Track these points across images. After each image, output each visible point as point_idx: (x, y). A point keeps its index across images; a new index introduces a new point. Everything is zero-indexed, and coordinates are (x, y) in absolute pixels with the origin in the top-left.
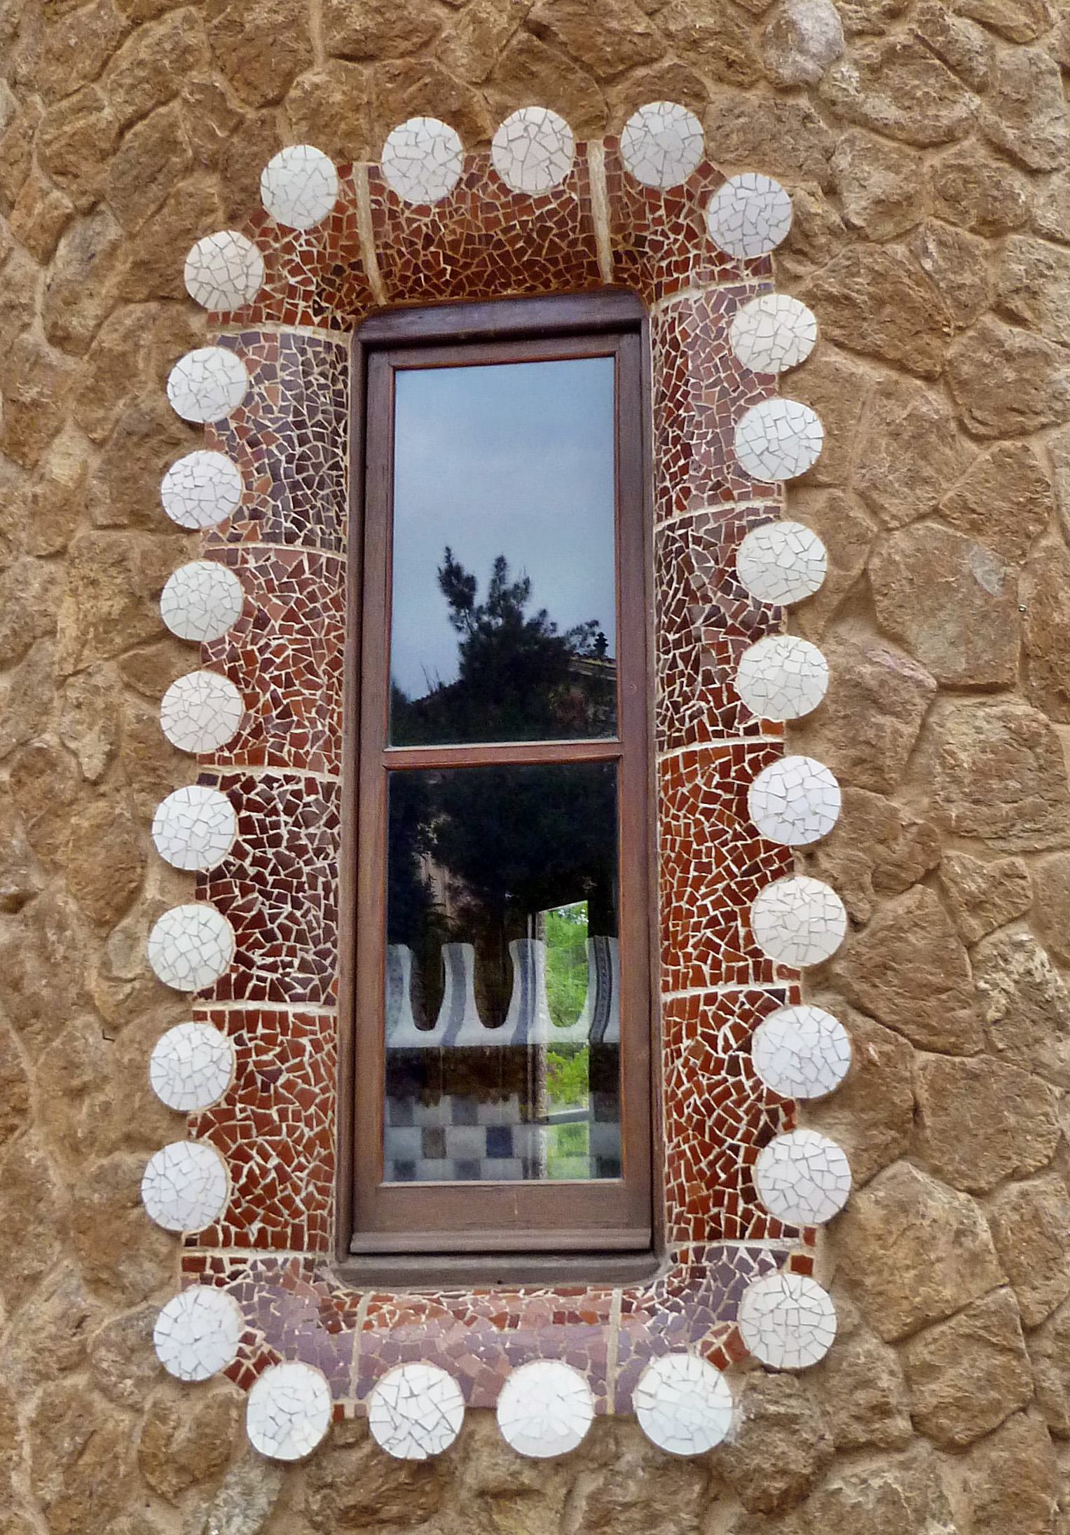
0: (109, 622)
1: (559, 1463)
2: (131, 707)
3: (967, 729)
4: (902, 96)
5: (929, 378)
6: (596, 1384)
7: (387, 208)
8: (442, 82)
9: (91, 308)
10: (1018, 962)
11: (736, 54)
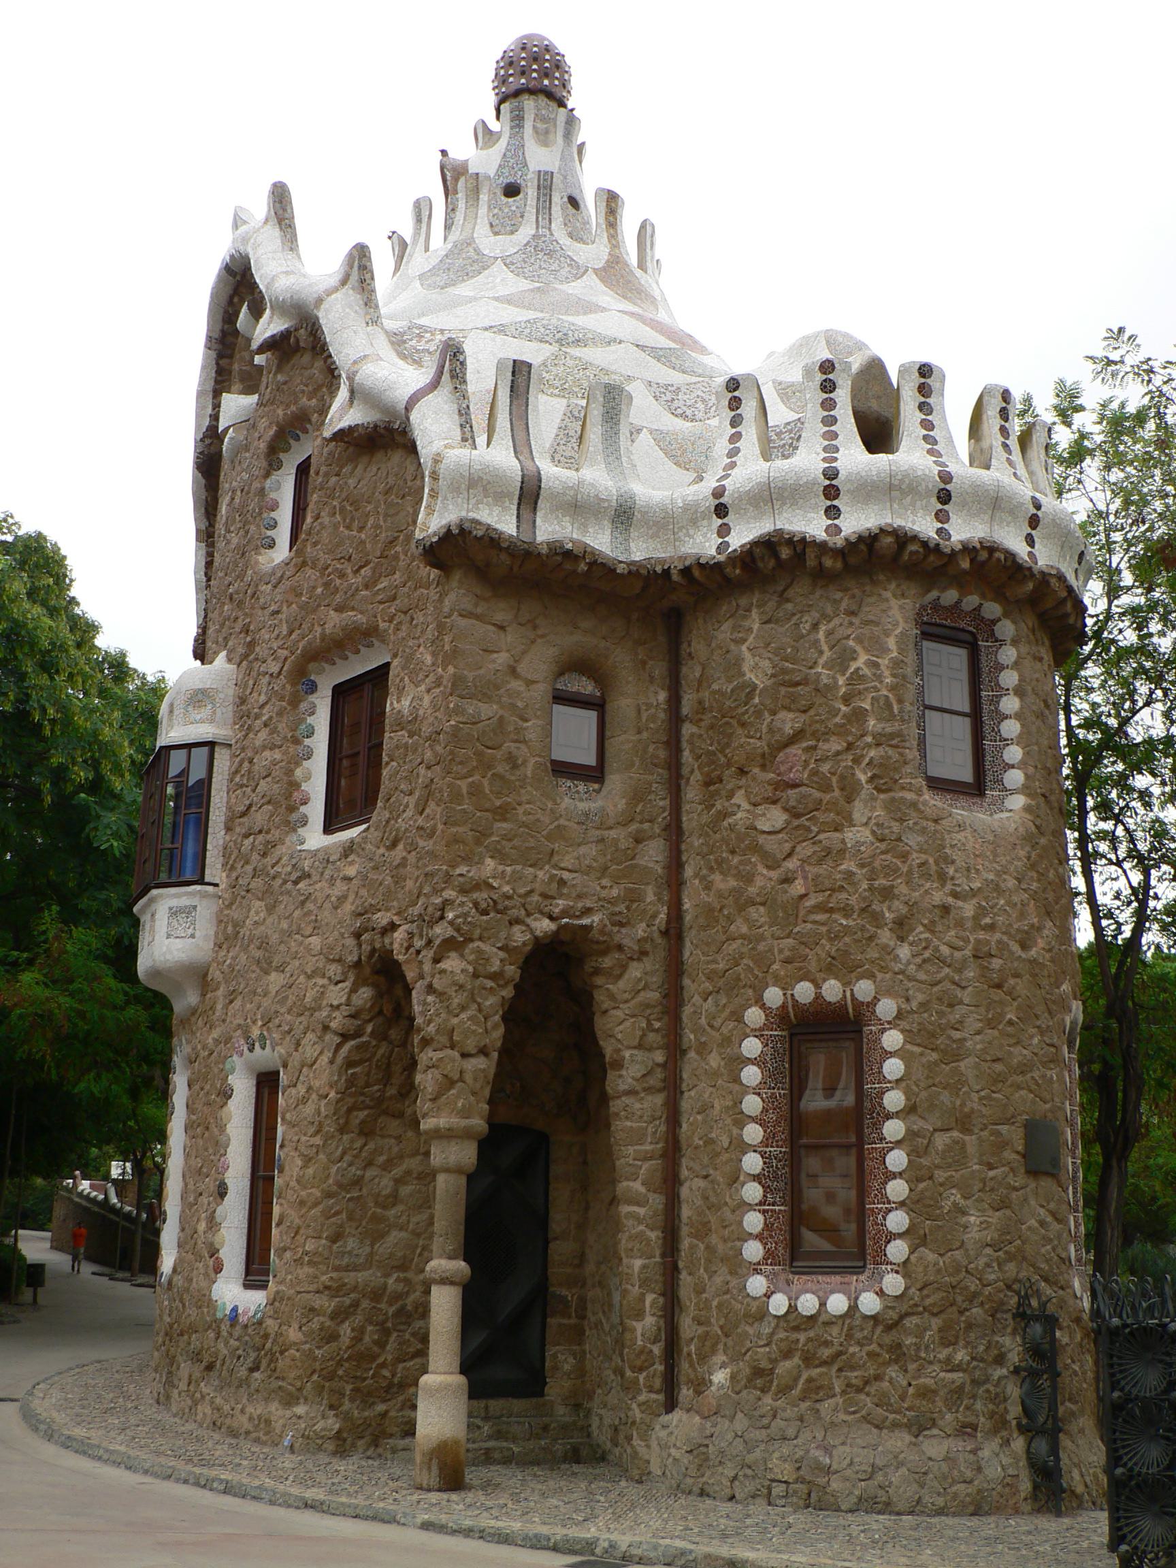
0: (728, 1108)
1: (841, 1316)
2: (735, 1131)
3: (941, 1140)
4: (927, 972)
5: (932, 1050)
6: (849, 1299)
7: (795, 1002)
8: (809, 971)
9: (720, 1021)
10: (952, 1198)
11: (883, 964)
